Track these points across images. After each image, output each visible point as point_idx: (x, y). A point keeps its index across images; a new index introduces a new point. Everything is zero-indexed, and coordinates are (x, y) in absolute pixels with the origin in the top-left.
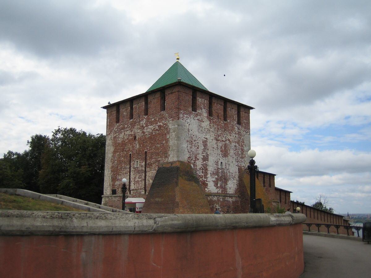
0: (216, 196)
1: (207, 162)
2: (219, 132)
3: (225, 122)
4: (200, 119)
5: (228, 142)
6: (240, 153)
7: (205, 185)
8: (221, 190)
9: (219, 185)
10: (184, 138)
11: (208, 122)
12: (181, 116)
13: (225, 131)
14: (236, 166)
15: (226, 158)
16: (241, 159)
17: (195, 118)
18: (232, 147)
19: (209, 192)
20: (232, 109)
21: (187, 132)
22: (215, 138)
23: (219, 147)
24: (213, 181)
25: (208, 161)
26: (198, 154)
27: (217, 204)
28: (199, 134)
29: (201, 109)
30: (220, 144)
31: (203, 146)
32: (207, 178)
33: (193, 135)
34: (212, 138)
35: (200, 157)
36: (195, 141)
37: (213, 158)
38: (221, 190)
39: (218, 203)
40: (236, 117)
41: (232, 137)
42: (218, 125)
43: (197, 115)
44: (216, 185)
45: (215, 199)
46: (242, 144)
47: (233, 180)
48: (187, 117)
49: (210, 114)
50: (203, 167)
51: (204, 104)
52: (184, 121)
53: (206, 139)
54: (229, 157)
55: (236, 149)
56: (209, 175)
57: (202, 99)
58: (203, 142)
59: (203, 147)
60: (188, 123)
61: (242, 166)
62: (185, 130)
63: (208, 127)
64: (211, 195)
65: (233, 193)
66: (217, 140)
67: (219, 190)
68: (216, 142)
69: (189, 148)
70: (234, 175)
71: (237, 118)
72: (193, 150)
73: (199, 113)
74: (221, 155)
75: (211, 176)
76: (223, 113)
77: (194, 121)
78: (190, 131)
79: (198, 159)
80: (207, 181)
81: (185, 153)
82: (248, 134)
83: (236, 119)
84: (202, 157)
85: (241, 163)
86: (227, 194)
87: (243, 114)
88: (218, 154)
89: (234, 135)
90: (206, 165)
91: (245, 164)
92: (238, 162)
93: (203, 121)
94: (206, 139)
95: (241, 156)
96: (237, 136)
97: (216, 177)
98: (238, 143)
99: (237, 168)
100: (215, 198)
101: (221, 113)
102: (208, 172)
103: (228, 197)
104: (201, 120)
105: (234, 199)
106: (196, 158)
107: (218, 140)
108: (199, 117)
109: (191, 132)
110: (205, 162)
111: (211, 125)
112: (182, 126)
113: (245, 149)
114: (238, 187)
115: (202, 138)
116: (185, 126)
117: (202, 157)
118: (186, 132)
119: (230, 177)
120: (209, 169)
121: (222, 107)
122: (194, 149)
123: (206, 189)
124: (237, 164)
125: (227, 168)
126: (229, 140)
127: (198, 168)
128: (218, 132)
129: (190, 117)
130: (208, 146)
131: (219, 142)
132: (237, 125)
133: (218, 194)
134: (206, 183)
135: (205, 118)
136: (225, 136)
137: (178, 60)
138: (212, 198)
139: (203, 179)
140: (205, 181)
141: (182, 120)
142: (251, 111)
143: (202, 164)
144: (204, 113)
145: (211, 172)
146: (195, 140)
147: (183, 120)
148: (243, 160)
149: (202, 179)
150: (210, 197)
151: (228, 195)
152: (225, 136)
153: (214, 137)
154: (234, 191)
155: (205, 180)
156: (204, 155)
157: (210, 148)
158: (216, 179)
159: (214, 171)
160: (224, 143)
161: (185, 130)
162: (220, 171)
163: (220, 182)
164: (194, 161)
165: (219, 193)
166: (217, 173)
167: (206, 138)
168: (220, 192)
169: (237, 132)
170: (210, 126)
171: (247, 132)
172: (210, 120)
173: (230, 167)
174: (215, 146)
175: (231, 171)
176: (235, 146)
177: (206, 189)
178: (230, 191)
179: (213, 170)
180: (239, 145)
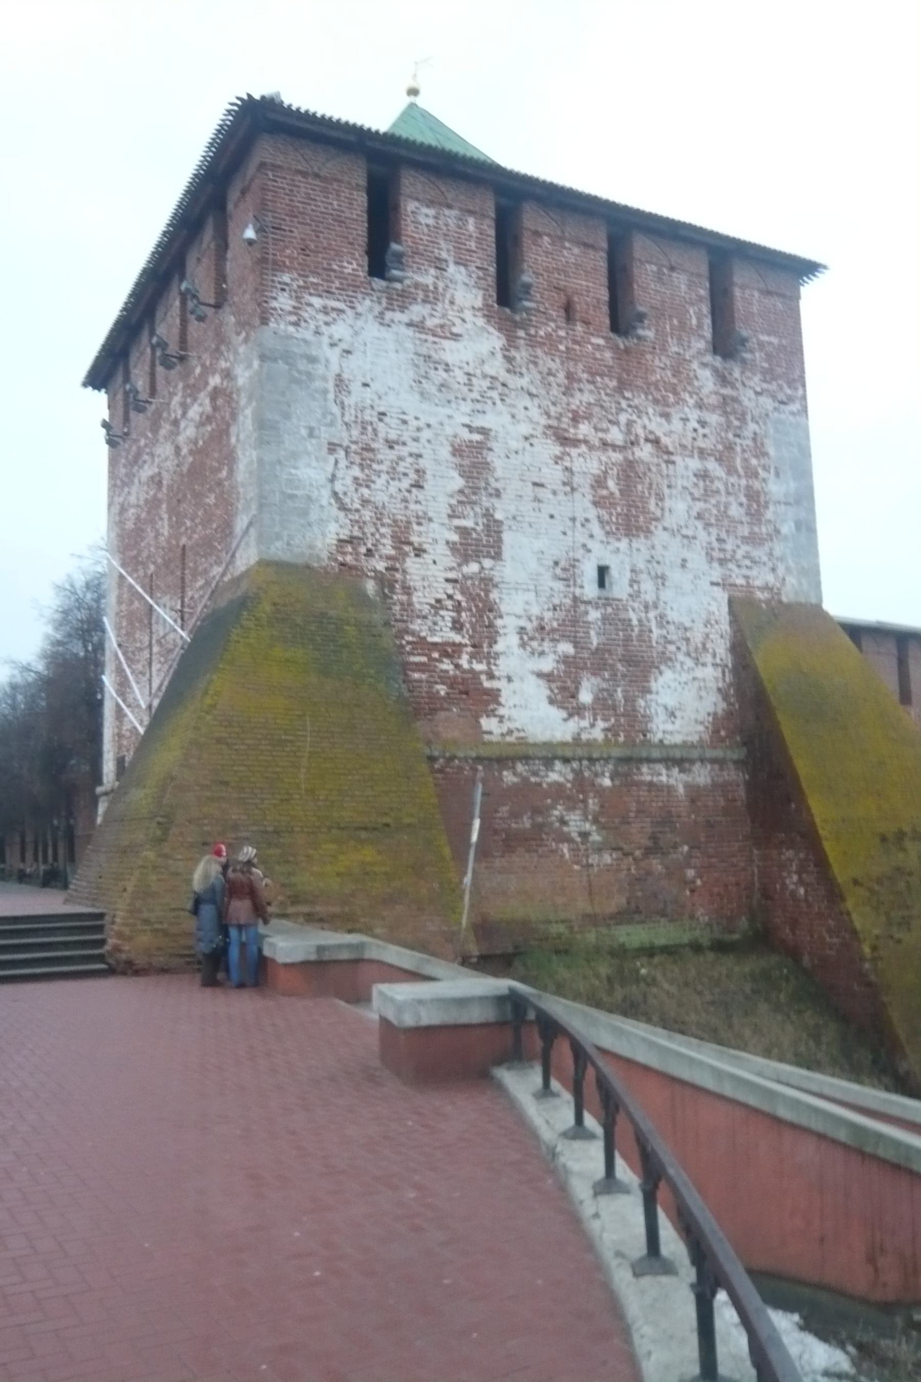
0: (566, 760)
1: (487, 563)
2: (583, 398)
3: (621, 342)
4: (430, 323)
5: (644, 452)
6: (735, 511)
7: (477, 696)
8: (601, 724)
9: (586, 697)
10: (304, 432)
11: (495, 340)
12: (284, 302)
13: (621, 388)
14: (713, 584)
15: (640, 543)
16: (745, 548)
17: (389, 315)
18: (680, 482)
19: (509, 739)
20: (672, 269)
21: (331, 396)
22: (549, 427)
23: (583, 482)
24: (540, 675)
25: (497, 556)
26: (423, 519)
27: (571, 809)
28: (425, 406)
29: (440, 265)
30: (588, 464)
31: (455, 474)
32: (491, 658)
33: (382, 409)
34: (524, 429)
35: (437, 535)
36: (391, 445)
37: (539, 544)
38: (601, 724)
39: (584, 801)
40: (699, 315)
41: (679, 426)
42: (569, 356)
43: (401, 300)
44: (563, 693)
45: (554, 777)
46: (754, 462)
47: (689, 663)
48: (325, 310)
49: (506, 292)
50: (458, 597)
52: (306, 333)
53: (477, 437)
54: (660, 536)
55: (708, 493)
56: (508, 642)
57: (447, 212)
58: (457, 451)
59: (459, 483)
60: (332, 345)
61: (758, 583)
62: (318, 384)
63: (497, 367)
64: (526, 759)
65: (695, 738)
66: (564, 440)
67: (585, 723)
68: (557, 450)
69: (344, 484)
70: (697, 637)
71: (708, 321)
72: (380, 498)
73: (417, 285)
75: (523, 645)
76: (604, 295)
77: (384, 333)
78: (356, 387)
79: (419, 552)
80: (491, 676)
81: (314, 516)
82: (795, 407)
83: (700, 326)
84: (455, 538)
85: (745, 572)
86: (646, 743)
87: (747, 295)
88: (573, 519)
89: (694, 415)
90: (487, 583)
91: (781, 570)
92: (722, 562)
93: (455, 330)
94: (477, 437)
95: (745, 531)
96: (714, 418)
97: (566, 648)
98: (725, 455)
99: (722, 596)
100: (558, 774)
101: (593, 290)
102: (499, 622)
103: (659, 761)
104: (442, 326)
105: (702, 776)
106: (401, 540)
107: (575, 443)
108: (417, 311)
109: (356, 396)
110: (473, 567)
111: (513, 353)
112: (287, 357)
113: (775, 488)
114: (729, 704)
115: (449, 430)
116: (313, 360)
117: (455, 538)
118: (325, 392)
119: (672, 648)
120: (504, 608)
121: (600, 261)
122: (384, 491)
123: (487, 723)
124: (716, 573)
125: (649, 597)
126: (656, 442)
127: (421, 600)
128: (568, 392)
129: (349, 312)
130: (499, 473)
131: (584, 448)
132: (708, 358)
133: (580, 752)
134: (487, 684)
135: (468, 315)
136: (623, 418)
137: (412, 99)
138: (535, 774)
139: (464, 662)
140: (475, 674)
141: (291, 329)
142: (811, 293)
143: (452, 575)
144: (465, 291)
145: (523, 623)
146: (393, 436)
147: (296, 324)
148: (759, 553)
149: (457, 666)
150: (520, 767)
151: (656, 754)
152: (623, 418)
153: (543, 421)
154: (701, 728)
155: (479, 667)
156: (468, 523)
157: (511, 488)
158: (565, 660)
159: (548, 615)
160: (617, 457)
161: (318, 384)
162: (594, 615)
163: (595, 680)
164: (389, 558)
165: (590, 744)
166: (570, 624)
167: (484, 431)
168: (597, 734)
169: (713, 400)
170: (509, 359)
171: (781, 396)
172: (508, 328)
173: (667, 595)
174: (553, 475)
175: (672, 616)
176: (703, 475)
177: (487, 723)
178: (669, 727)
179: (535, 611)
180: (732, 470)
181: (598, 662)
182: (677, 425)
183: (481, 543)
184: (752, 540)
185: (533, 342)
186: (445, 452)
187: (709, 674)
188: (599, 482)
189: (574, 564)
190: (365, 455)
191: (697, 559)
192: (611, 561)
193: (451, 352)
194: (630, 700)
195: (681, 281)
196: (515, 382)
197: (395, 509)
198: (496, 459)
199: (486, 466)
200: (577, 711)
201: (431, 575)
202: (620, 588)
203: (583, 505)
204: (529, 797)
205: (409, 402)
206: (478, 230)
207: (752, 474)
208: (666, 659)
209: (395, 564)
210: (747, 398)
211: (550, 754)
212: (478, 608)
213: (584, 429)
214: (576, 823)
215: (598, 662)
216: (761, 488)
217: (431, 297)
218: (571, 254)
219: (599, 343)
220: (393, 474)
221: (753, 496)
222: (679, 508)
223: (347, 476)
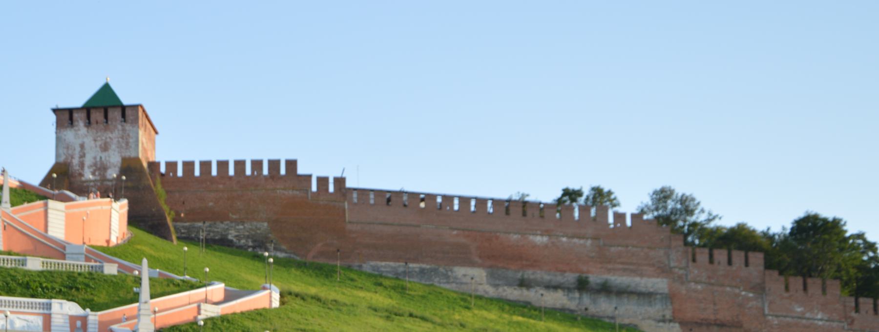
30: (99, 143)
44: (93, 174)
54: (110, 151)
87: (128, 112)
98: (122, 138)
122: (70, 152)
144: (81, 124)
166: (95, 164)
181: (99, 169)
183: (83, 156)
190: (68, 148)
191: (116, 153)
193: (79, 132)
201: (76, 161)
202: (103, 159)
203: (98, 149)
204: (88, 187)
206: (83, 115)
211: (91, 181)
212: (82, 165)
215: (99, 169)
216: (129, 141)
218: (98, 114)
219: (102, 126)
222: (113, 147)
223: (65, 151)
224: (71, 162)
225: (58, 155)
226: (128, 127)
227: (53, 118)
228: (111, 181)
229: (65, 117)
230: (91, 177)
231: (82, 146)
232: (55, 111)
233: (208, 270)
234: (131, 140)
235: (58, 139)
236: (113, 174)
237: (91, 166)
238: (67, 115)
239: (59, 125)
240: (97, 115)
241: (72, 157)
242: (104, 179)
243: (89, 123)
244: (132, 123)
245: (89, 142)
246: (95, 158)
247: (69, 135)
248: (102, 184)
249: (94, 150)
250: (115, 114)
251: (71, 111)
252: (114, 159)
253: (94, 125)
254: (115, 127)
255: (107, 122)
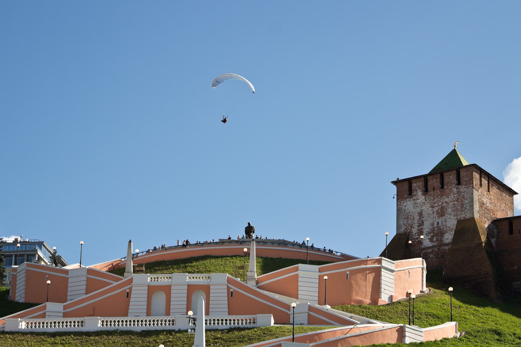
9: (434, 240)
11: (424, 197)
15: (443, 217)
30: (435, 209)
35: (416, 225)
44: (431, 240)
51: (419, 187)
54: (446, 215)
58: (418, 214)
59: (418, 217)
66: (433, 207)
74: (437, 218)
90: (422, 229)
99: (456, 221)
121: (439, 180)
122: (410, 222)
126: (446, 202)
128: (433, 200)
144: (420, 193)
166: (433, 231)
182: (450, 198)
183: (421, 224)
184: (462, 211)
185: (429, 195)
186: (417, 214)
187: (453, 232)
188: (438, 211)
189: (433, 223)
191: (452, 217)
192: (439, 221)
193: (418, 201)
194: (441, 239)
195: (451, 177)
196: (426, 202)
197: (411, 223)
198: (424, 213)
199: (422, 214)
200: (433, 242)
201: (415, 230)
202: (440, 225)
203: (435, 215)
205: (413, 210)
206: (421, 184)
207: (462, 201)
208: (446, 232)
209: (411, 230)
210: (462, 190)
211: (429, 248)
213: (436, 204)
214: (431, 256)
215: (437, 235)
217: (415, 195)
218: (435, 180)
219: (438, 192)
220: (411, 219)
221: (462, 204)
224: (411, 232)
225: (398, 227)
226: (462, 188)
227: (394, 188)
228: (447, 245)
229: (405, 188)
230: (430, 244)
231: (420, 214)
232: (394, 183)
233: (49, 282)
234: (466, 202)
235: (399, 211)
236: (448, 237)
237: (429, 233)
238: (406, 186)
239: (400, 197)
240: (434, 182)
241: (412, 227)
242: (441, 244)
243: (426, 191)
244: (465, 185)
245: (427, 209)
246: (432, 224)
247: (409, 205)
248: (439, 249)
249: (436, 217)
250: (450, 177)
251: (410, 181)
252: (451, 222)
253: (431, 192)
254: (451, 190)
255: (442, 187)
